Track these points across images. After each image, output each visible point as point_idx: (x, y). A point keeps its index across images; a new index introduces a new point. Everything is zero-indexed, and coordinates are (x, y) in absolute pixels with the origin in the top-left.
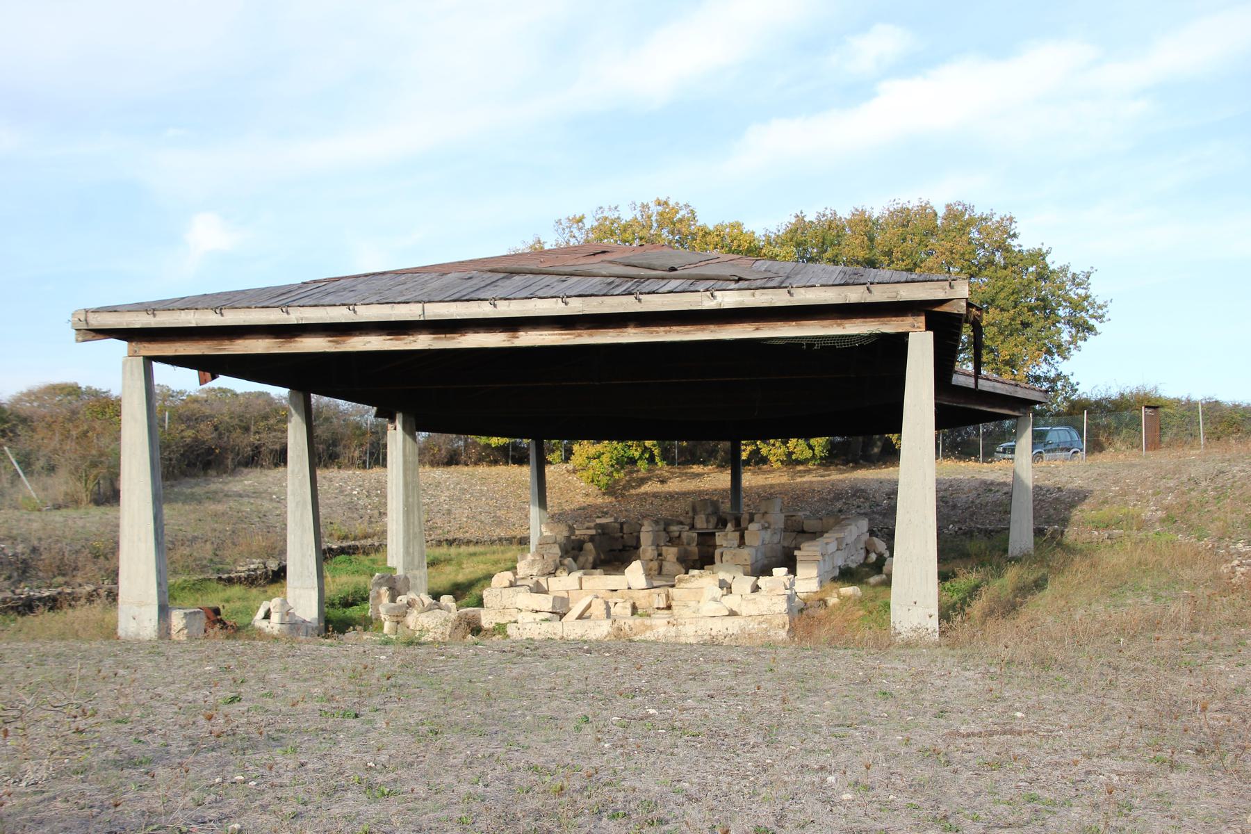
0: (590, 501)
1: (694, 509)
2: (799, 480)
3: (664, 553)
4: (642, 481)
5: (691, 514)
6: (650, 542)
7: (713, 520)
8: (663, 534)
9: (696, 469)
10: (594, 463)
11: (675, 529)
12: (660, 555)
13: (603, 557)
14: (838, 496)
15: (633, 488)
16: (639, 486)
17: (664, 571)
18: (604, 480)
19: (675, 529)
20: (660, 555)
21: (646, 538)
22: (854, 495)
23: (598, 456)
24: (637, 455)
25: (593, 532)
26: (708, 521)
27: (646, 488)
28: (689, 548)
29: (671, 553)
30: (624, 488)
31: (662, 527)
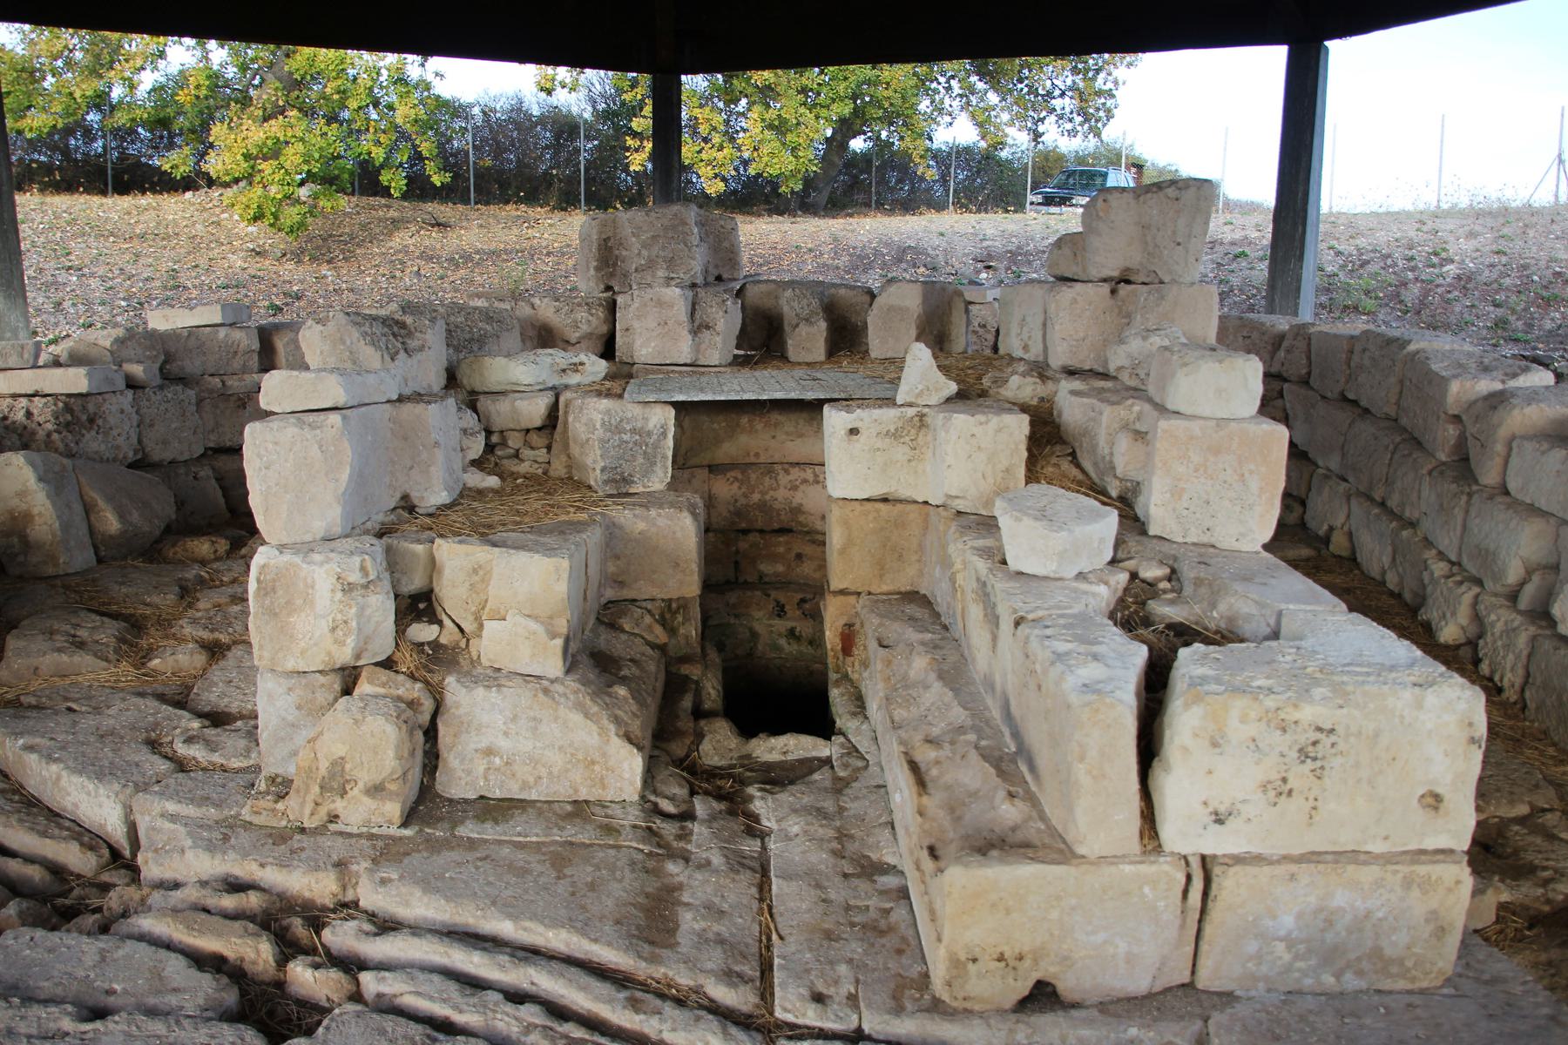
3: (452, 595)
4: (396, 224)
6: (327, 514)
8: (443, 420)
10: (267, 167)
11: (520, 377)
12: (417, 605)
13: (111, 523)
16: (390, 234)
17: (463, 776)
18: (291, 214)
19: (520, 377)
20: (417, 605)
23: (274, 151)
24: (379, 154)
25: (75, 381)
27: (401, 239)
28: (630, 519)
29: (516, 596)
31: (428, 369)
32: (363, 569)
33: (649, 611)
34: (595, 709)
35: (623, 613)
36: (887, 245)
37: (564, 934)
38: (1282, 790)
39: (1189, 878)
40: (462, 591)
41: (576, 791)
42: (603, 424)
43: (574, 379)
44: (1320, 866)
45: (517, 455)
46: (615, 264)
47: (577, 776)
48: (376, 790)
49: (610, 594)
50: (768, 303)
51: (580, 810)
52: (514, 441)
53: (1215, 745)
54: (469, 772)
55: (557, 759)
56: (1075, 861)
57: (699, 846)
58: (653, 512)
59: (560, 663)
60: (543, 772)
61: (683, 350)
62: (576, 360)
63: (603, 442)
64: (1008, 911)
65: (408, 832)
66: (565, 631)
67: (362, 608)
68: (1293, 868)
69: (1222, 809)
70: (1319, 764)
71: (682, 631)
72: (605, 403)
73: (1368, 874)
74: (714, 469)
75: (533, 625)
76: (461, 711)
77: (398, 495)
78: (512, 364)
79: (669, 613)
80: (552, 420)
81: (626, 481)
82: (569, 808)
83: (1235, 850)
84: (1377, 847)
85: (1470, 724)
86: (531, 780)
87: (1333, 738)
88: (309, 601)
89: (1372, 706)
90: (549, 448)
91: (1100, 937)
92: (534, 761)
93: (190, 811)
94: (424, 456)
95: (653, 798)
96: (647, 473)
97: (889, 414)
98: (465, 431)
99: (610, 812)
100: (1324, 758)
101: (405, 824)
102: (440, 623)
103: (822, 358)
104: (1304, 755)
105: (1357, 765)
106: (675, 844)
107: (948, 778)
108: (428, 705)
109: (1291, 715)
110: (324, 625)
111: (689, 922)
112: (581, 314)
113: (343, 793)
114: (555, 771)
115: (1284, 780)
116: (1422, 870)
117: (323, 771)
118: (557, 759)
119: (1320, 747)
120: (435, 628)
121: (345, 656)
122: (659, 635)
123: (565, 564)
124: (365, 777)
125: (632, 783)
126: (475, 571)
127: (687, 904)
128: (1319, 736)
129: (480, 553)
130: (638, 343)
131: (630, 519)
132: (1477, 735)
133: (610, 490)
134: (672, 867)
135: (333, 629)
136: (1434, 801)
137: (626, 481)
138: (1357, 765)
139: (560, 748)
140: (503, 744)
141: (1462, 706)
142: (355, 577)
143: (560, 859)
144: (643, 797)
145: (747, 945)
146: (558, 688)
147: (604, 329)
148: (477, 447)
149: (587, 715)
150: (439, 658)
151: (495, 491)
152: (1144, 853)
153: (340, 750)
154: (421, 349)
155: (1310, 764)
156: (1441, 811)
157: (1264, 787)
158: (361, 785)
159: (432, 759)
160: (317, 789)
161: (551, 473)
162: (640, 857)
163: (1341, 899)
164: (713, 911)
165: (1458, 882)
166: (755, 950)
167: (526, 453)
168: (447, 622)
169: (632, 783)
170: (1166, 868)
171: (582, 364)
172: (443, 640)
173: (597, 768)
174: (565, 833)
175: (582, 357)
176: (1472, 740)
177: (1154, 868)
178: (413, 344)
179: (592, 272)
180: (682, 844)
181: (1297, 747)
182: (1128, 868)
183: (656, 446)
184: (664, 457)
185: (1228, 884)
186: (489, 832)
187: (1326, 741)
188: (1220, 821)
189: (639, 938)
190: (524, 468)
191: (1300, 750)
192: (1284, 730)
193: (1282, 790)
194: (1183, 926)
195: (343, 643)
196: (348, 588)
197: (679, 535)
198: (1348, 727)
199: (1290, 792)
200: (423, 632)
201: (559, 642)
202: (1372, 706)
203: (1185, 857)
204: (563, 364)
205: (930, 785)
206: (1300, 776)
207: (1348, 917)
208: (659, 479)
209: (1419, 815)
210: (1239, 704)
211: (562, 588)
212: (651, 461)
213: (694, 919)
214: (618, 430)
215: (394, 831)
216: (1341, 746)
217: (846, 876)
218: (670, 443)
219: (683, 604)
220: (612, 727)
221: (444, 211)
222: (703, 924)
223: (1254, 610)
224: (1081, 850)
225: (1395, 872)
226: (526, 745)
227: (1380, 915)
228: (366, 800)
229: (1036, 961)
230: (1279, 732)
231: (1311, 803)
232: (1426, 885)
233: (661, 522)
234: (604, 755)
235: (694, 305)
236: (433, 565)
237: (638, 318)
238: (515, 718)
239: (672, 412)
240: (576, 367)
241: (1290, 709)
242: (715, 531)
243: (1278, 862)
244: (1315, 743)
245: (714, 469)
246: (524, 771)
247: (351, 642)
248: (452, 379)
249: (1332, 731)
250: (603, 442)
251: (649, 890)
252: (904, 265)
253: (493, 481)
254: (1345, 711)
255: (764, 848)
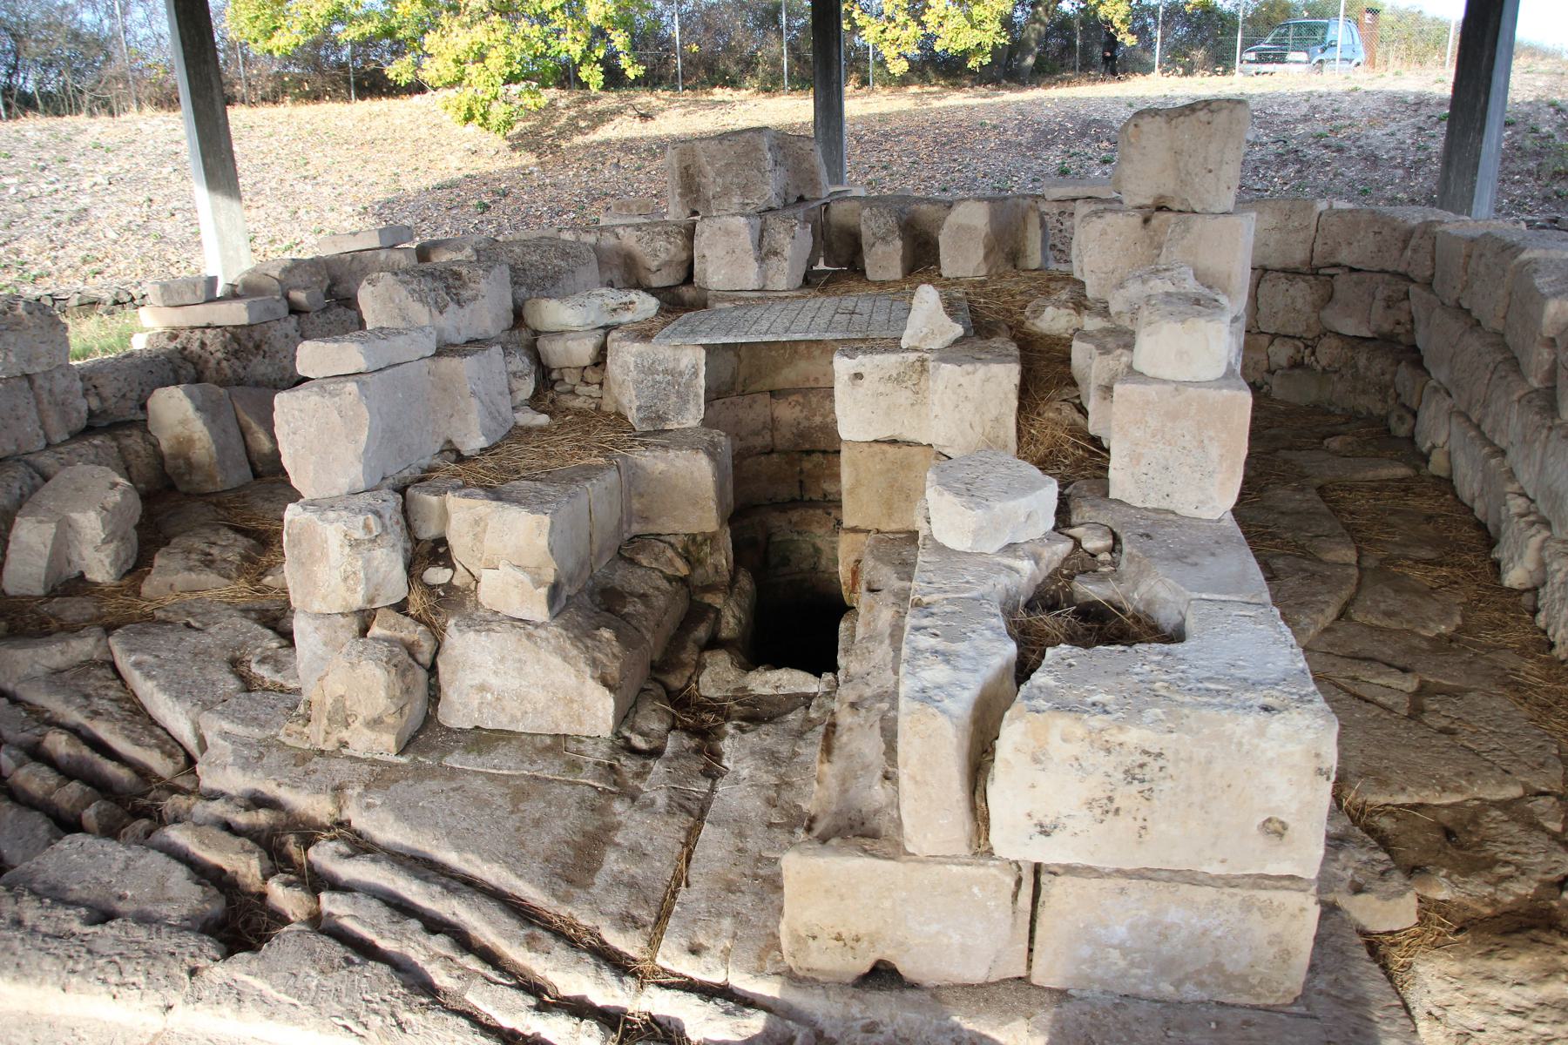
0: (481, 165)
1: (690, 184)
2: (936, 104)
3: (460, 545)
5: (674, 211)
7: (794, 243)
9: (719, 93)
11: (569, 319)
14: (1045, 136)
15: (581, 131)
17: (459, 710)
20: (428, 552)
21: (321, 433)
22: (1082, 134)
26: (765, 252)
29: (507, 547)
30: (561, 133)
32: (366, 527)
33: (672, 545)
34: (575, 652)
35: (642, 549)
36: (1072, 118)
37: (496, 868)
38: (1108, 808)
39: (1019, 882)
40: (468, 540)
41: (557, 726)
42: (636, 365)
43: (626, 317)
44: (1152, 883)
45: (572, 392)
46: (698, 191)
47: (558, 712)
48: (375, 723)
49: (636, 528)
50: (850, 220)
51: (558, 744)
52: (571, 379)
53: (1036, 760)
54: (466, 706)
55: (541, 697)
56: (905, 858)
57: (650, 786)
58: (672, 454)
59: (546, 609)
60: (529, 707)
61: (749, 277)
62: (625, 299)
63: (636, 382)
64: (842, 898)
65: (403, 760)
66: (552, 579)
67: (368, 562)
68: (1123, 882)
69: (1047, 821)
70: (1146, 786)
71: (710, 561)
72: (638, 347)
73: (1204, 894)
74: (774, 394)
75: (521, 575)
76: (457, 652)
77: (441, 441)
78: (562, 307)
79: (692, 548)
80: (600, 358)
81: (662, 418)
82: (548, 741)
83: (1064, 861)
84: (1215, 869)
85: (1317, 755)
86: (519, 714)
87: (1161, 762)
88: (325, 555)
89: (1206, 731)
90: (601, 384)
91: (934, 927)
92: (521, 698)
93: (238, 729)
94: (462, 405)
95: (627, 734)
96: (680, 412)
97: (890, 361)
98: (514, 374)
99: (582, 747)
100: (1152, 780)
101: (401, 753)
102: (453, 568)
103: (899, 276)
104: (1130, 776)
105: (1189, 789)
106: (630, 782)
107: (853, 746)
108: (427, 647)
109: (1115, 736)
110: (337, 576)
111: (613, 862)
112: (660, 243)
113: (347, 725)
114: (539, 706)
115: (1110, 799)
116: (1263, 895)
117: (328, 707)
118: (541, 697)
119: (1147, 770)
120: (449, 572)
121: (358, 601)
122: (682, 569)
123: (547, 520)
124: (364, 712)
125: (605, 721)
126: (477, 523)
127: (618, 845)
128: (1145, 759)
129: (483, 507)
130: (710, 270)
131: (653, 461)
132: (1325, 766)
133: (646, 427)
134: (618, 806)
135: (345, 579)
136: (1275, 829)
137: (662, 418)
138: (1189, 789)
139: (544, 687)
140: (494, 681)
141: (1310, 735)
142: (359, 534)
143: (520, 793)
144: (617, 734)
145: (654, 889)
146: (542, 633)
147: (684, 256)
148: (527, 387)
149: (565, 659)
150: (452, 599)
151: (542, 430)
152: (975, 854)
153: (340, 690)
154: (475, 298)
155: (1136, 786)
156: (1285, 839)
157: (1090, 804)
158: (360, 718)
159: (434, 694)
160: (325, 721)
161: (604, 408)
162: (592, 794)
163: (1174, 915)
164: (637, 853)
165: (1302, 910)
166: (660, 895)
167: (581, 389)
168: (458, 566)
169: (605, 721)
170: (993, 871)
171: (632, 303)
172: (456, 582)
173: (575, 706)
174: (536, 767)
175: (633, 296)
176: (1320, 772)
177: (982, 871)
178: (466, 294)
179: (677, 198)
180: (636, 783)
181: (1122, 769)
182: (955, 869)
183: (688, 386)
184: (697, 395)
185: (1054, 890)
186: (472, 763)
187: (1154, 765)
188: (1046, 833)
189: (560, 876)
190: (578, 403)
191: (1126, 772)
192: (1108, 751)
193: (1108, 808)
194: (1014, 925)
195: (354, 591)
196: (355, 544)
197: (696, 474)
198: (1177, 752)
199: (1117, 811)
200: (437, 575)
201: (544, 591)
202: (1206, 731)
203: (1016, 862)
204: (613, 304)
205: (836, 752)
206: (1127, 796)
207: (1184, 933)
208: (692, 417)
209: (1259, 842)
210: (1063, 722)
211: (543, 542)
212: (683, 399)
213: (616, 861)
214: (651, 370)
215: (392, 758)
216: (1171, 770)
217: (770, 825)
218: (702, 382)
219: (711, 538)
220: (588, 670)
221: (644, 98)
222: (622, 866)
223: (1170, 597)
224: (910, 849)
225: (1232, 895)
226: (513, 683)
227: (1219, 933)
228: (367, 732)
229: (872, 943)
230: (1102, 753)
231: (1140, 823)
232: (1267, 911)
233: (680, 463)
234: (581, 694)
235: (762, 231)
236: (445, 516)
237: (709, 246)
238: (502, 660)
239: (703, 353)
240: (626, 306)
241: (1114, 731)
242: (779, 452)
243: (1109, 875)
244: (1142, 766)
245: (774, 394)
246: (512, 706)
247: (361, 590)
248: (518, 316)
249: (1160, 755)
250: (637, 383)
251: (589, 828)
252: (1087, 140)
253: (543, 419)
254: (1174, 736)
255: (712, 790)
